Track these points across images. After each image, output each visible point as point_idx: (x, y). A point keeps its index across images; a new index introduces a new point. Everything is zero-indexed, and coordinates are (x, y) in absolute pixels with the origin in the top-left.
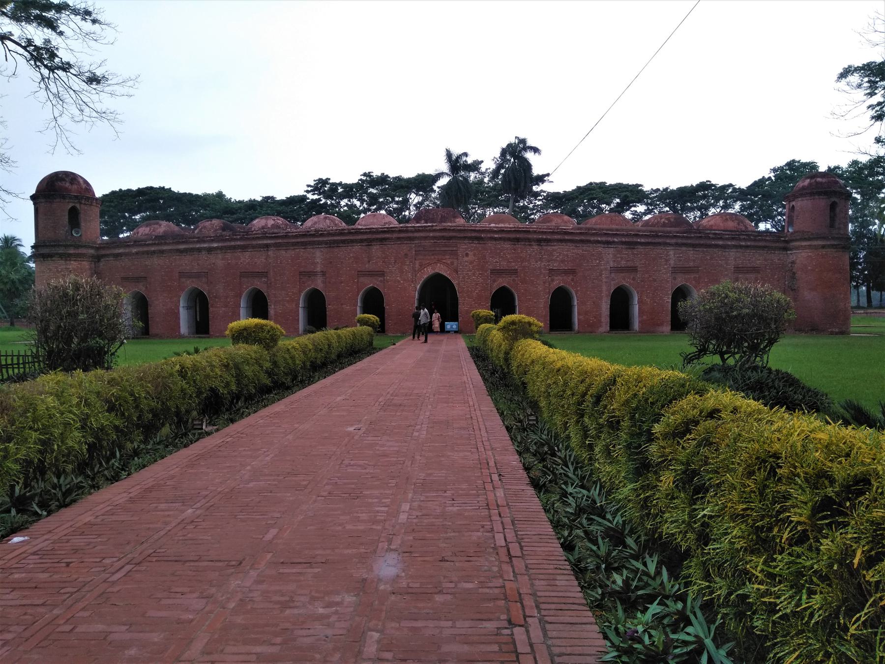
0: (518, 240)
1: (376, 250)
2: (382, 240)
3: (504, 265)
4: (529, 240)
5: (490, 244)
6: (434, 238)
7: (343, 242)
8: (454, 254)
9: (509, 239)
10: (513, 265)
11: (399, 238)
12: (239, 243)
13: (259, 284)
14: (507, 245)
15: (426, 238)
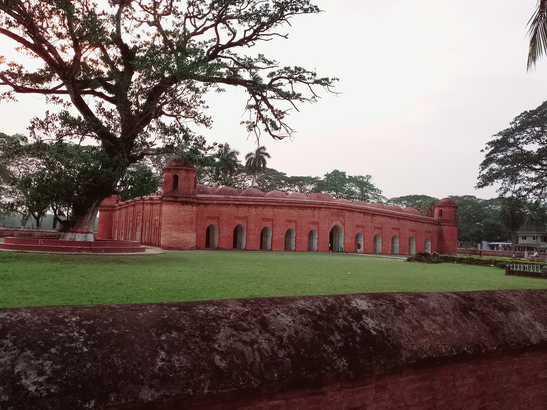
0: (365, 213)
1: (316, 211)
2: (320, 208)
3: (360, 223)
4: (369, 213)
5: (356, 214)
6: (338, 209)
7: (305, 207)
8: (344, 216)
9: (363, 213)
10: (364, 224)
11: (326, 208)
12: (262, 203)
13: (268, 225)
14: (362, 215)
15: (335, 209)
